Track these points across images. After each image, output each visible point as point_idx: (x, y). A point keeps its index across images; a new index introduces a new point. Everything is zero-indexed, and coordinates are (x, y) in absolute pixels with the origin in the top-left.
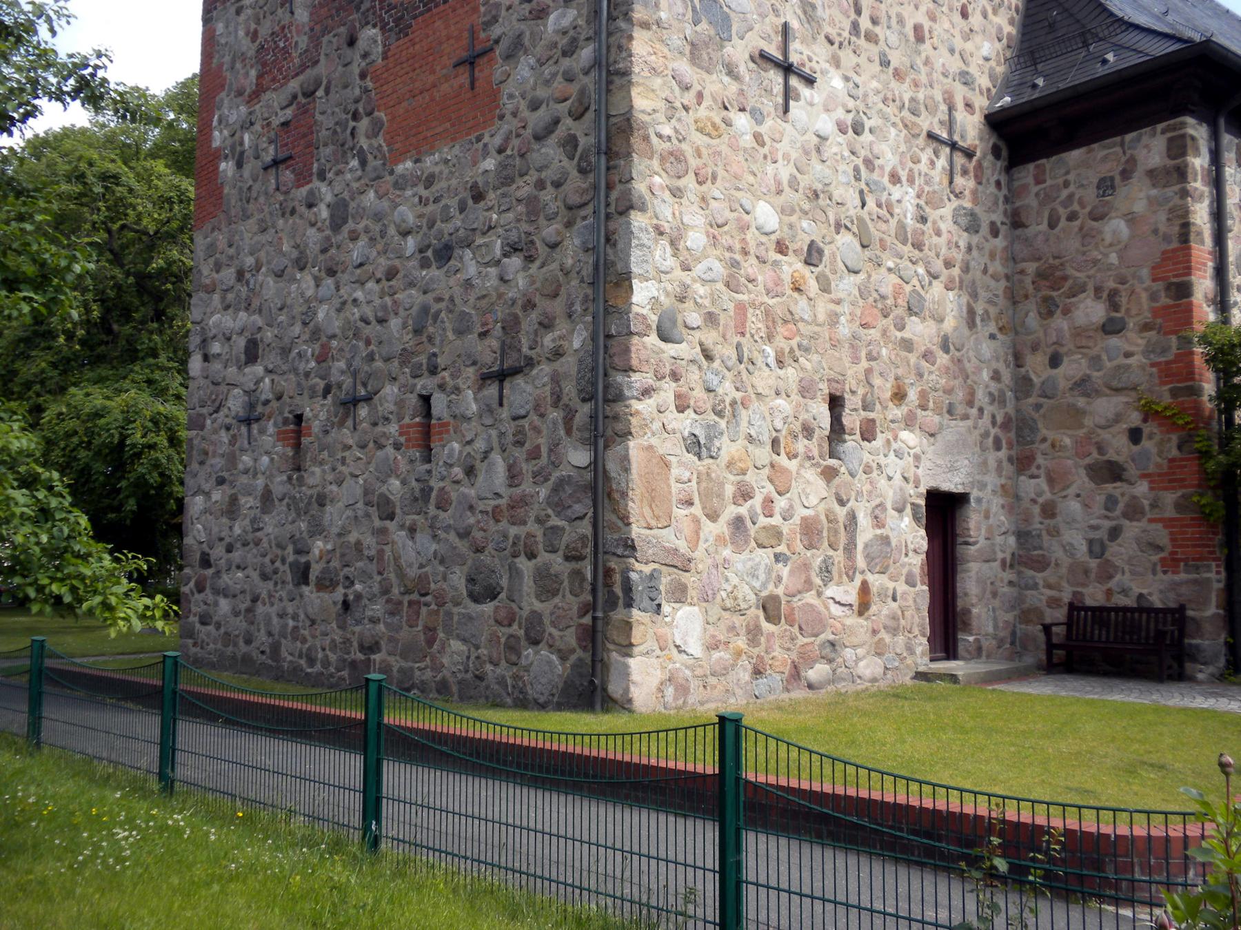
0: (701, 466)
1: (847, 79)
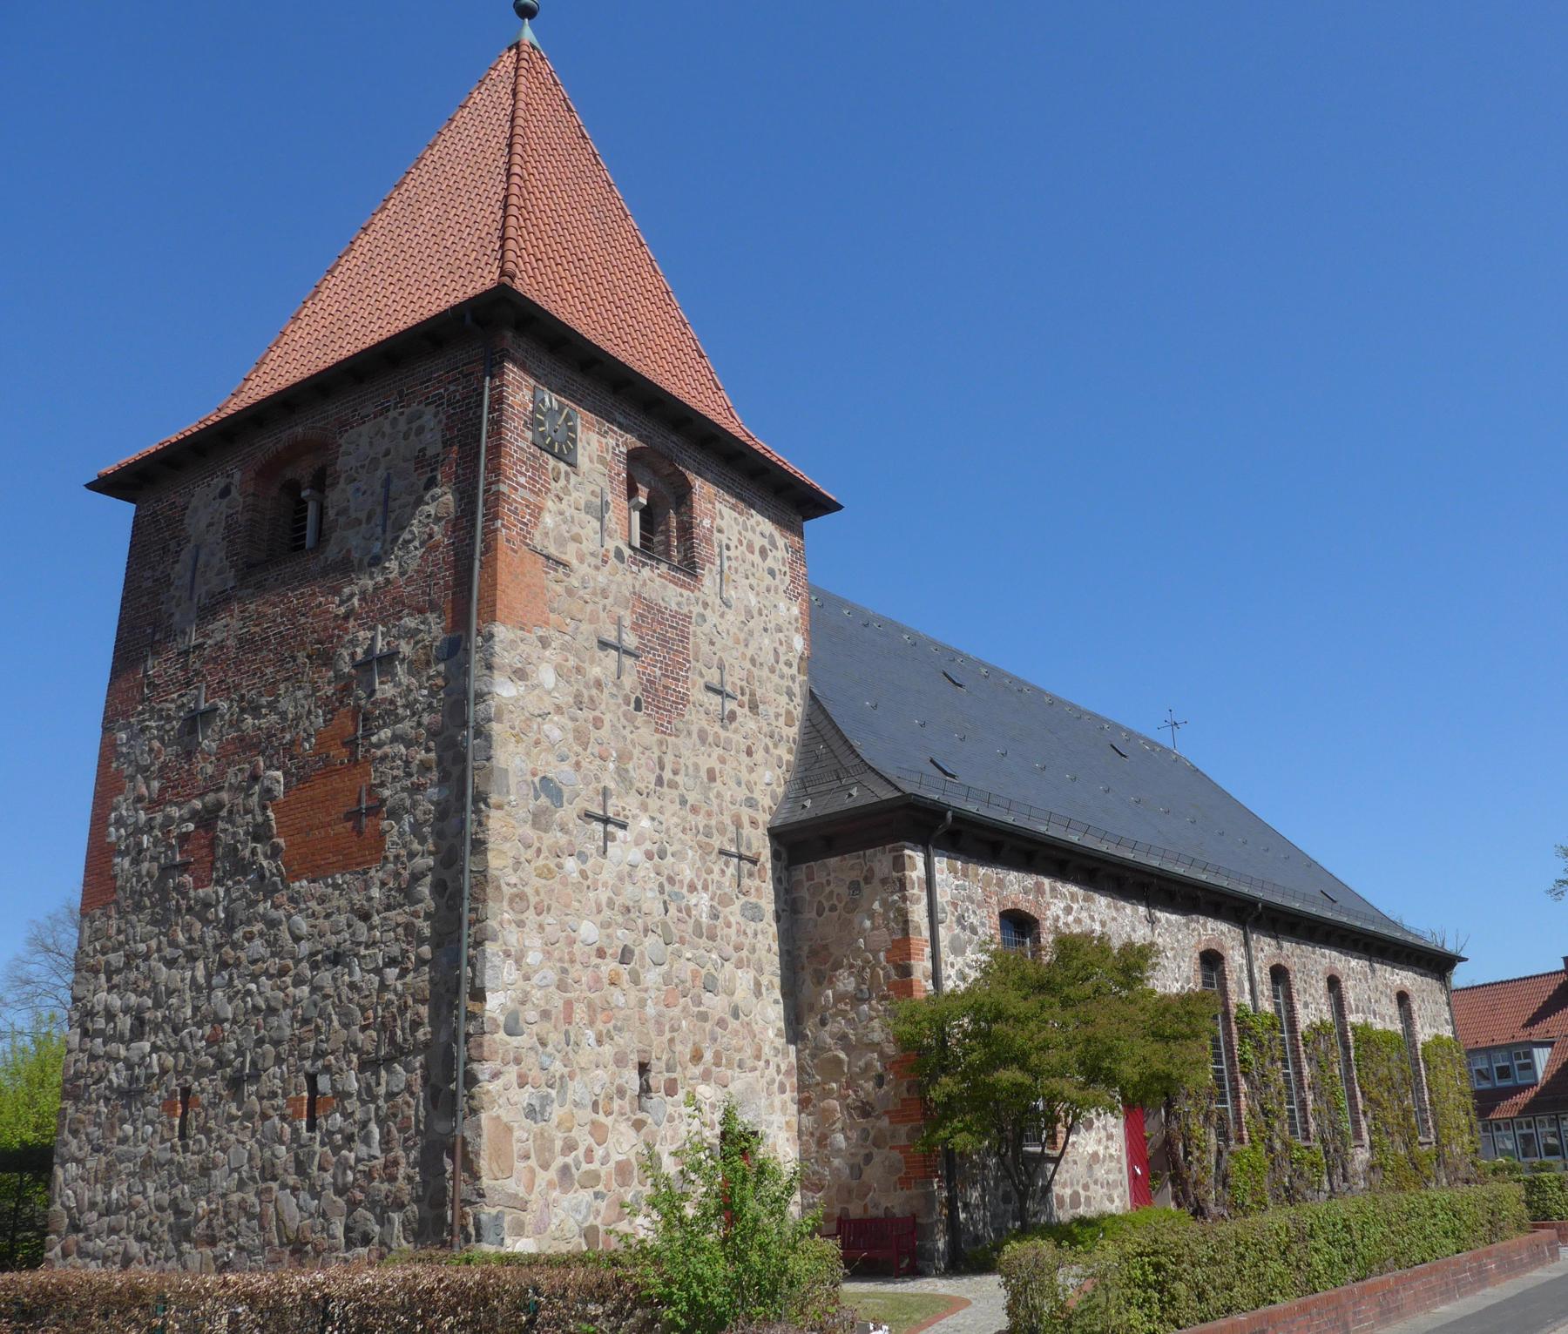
0: (535, 1127)
1: (653, 819)
